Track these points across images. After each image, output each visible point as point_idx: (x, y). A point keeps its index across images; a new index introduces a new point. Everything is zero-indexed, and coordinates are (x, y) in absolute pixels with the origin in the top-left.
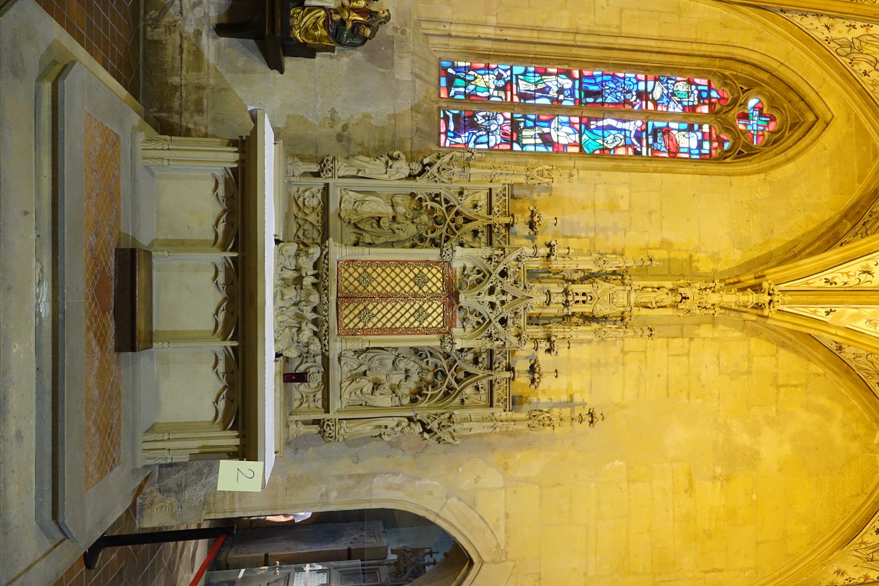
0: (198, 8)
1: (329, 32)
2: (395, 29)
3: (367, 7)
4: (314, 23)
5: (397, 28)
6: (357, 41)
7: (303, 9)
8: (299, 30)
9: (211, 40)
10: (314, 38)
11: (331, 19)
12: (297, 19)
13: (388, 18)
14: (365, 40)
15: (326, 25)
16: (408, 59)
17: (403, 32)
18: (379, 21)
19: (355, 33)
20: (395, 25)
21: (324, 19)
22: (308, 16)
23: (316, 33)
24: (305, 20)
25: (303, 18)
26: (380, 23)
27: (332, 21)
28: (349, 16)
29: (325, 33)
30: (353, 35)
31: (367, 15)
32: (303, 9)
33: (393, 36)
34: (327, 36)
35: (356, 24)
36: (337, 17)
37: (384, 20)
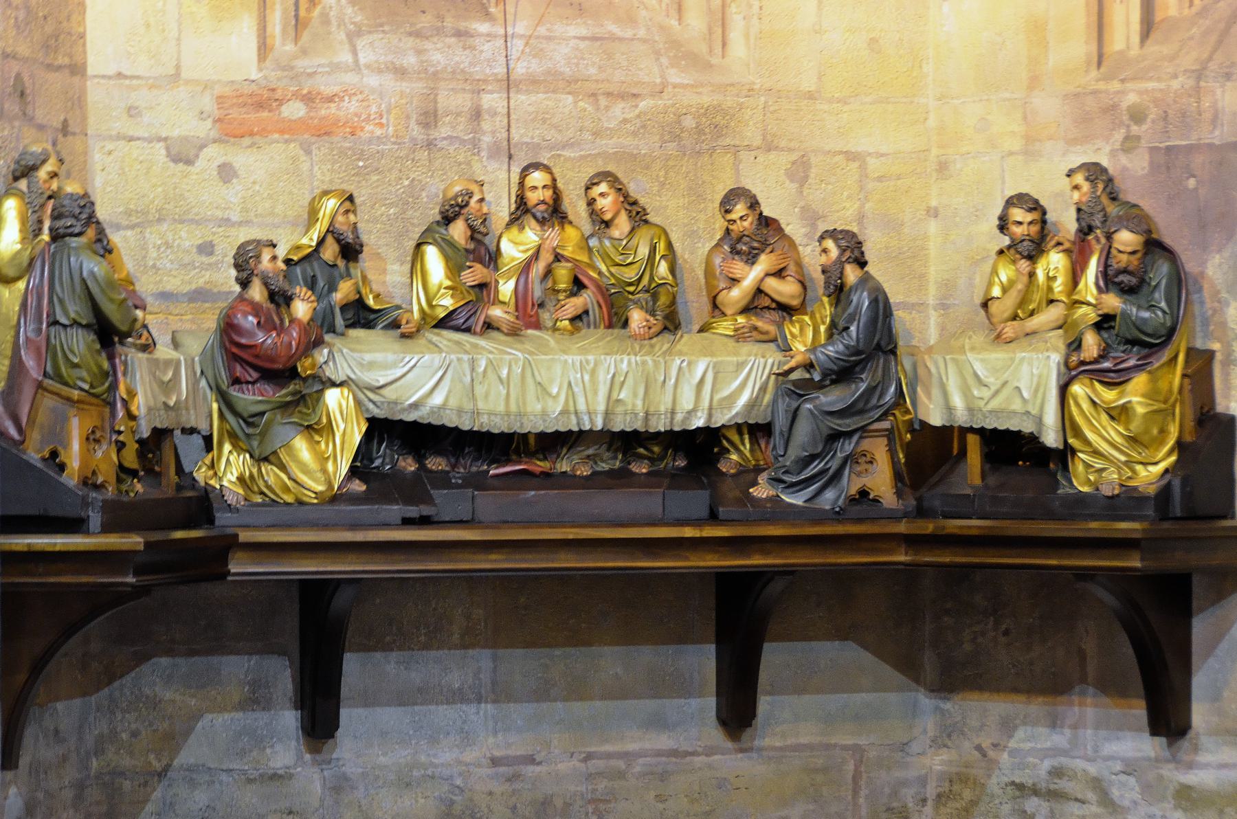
0: (1115, 793)
1: (1138, 368)
2: (1129, 144)
3: (1067, 245)
4: (1112, 418)
5: (1127, 138)
6: (1161, 272)
7: (1074, 452)
8: (1139, 468)
9: (1203, 758)
10: (1160, 415)
11: (1096, 361)
12: (1103, 470)
13: (1095, 172)
14: (1154, 246)
15: (1115, 378)
16: (1219, 92)
17: (1137, 116)
18: (1105, 200)
19: (1134, 281)
20: (1118, 145)
21: (1097, 384)
22: (1090, 435)
23: (1140, 410)
24: (1104, 447)
25: (1096, 453)
26: (1114, 198)
27: (1102, 357)
28: (1089, 304)
29: (1140, 381)
30: (1145, 290)
31: (1089, 242)
32: (1074, 452)
33: (1153, 150)
34: (1150, 372)
35: (1108, 280)
36: (1091, 344)
37: (1101, 186)
